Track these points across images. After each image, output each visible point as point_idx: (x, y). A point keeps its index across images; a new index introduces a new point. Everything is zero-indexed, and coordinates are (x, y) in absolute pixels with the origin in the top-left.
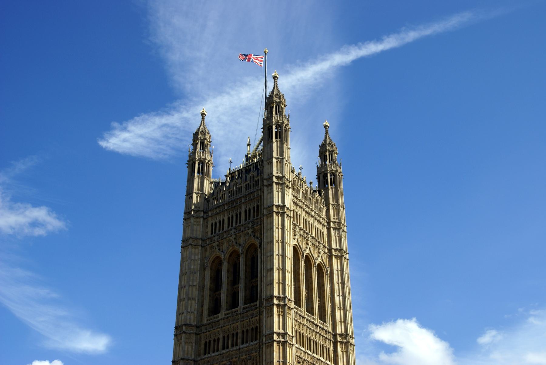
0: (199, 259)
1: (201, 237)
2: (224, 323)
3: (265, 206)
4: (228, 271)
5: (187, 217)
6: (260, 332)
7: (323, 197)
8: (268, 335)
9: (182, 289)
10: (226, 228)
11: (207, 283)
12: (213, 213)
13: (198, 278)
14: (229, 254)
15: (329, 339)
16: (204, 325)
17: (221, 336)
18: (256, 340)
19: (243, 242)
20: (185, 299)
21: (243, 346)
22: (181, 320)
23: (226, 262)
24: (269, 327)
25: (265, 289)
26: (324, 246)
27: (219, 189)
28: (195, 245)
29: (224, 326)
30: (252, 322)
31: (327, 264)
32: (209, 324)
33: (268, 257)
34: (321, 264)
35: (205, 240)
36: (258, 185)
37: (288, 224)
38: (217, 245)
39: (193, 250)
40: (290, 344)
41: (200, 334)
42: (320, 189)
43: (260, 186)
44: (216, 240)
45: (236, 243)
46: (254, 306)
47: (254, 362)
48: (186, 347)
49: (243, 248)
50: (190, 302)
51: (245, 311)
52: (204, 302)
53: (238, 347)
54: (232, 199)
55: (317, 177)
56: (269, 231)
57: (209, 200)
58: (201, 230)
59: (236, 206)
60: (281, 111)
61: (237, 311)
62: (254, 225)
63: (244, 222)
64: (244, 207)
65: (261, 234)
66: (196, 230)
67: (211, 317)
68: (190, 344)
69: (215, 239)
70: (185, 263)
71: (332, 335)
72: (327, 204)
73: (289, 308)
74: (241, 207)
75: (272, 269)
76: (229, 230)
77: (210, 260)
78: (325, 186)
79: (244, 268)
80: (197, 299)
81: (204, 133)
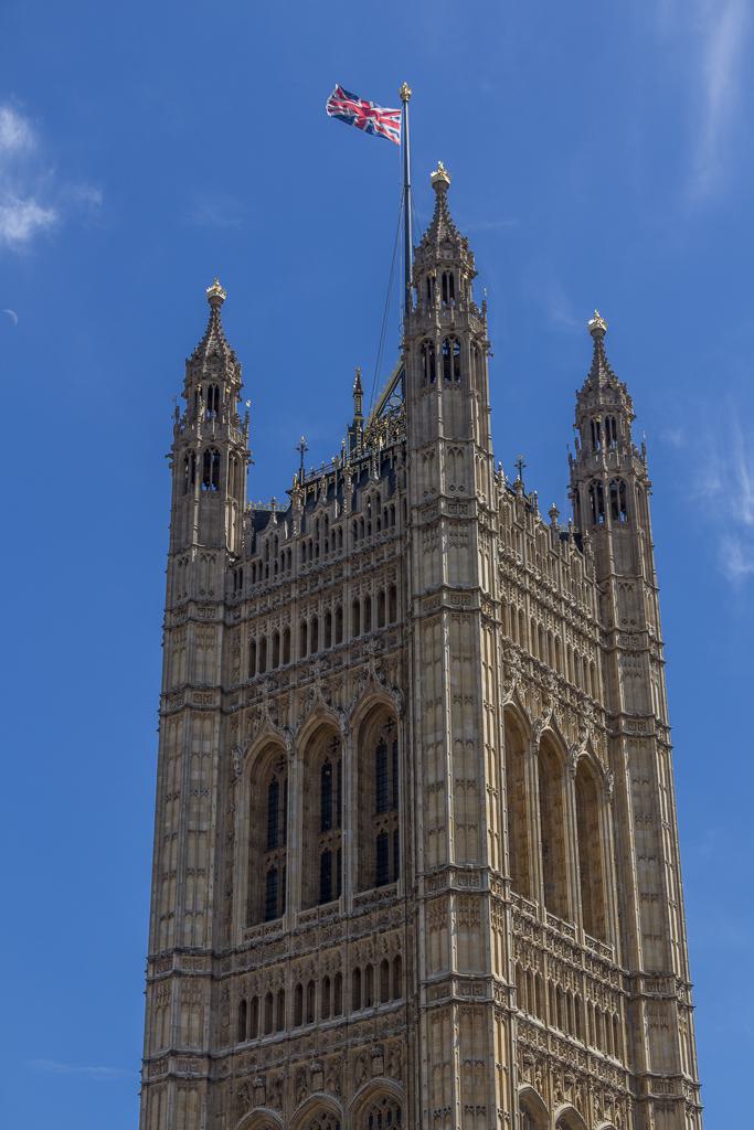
0: (216, 752)
1: (219, 684)
2: (298, 946)
3: (417, 592)
4: (306, 789)
5: (173, 620)
6: (409, 974)
7: (592, 553)
8: (434, 983)
9: (168, 844)
10: (295, 658)
11: (242, 823)
12: (255, 610)
13: (214, 810)
14: (308, 736)
15: (614, 991)
16: (236, 952)
17: (289, 986)
18: (397, 997)
19: (350, 701)
20: (175, 872)
21: (357, 1015)
22: (167, 936)
23: (299, 760)
24: (435, 958)
25: (421, 846)
26: (597, 709)
27: (272, 534)
28: (203, 710)
29: (297, 956)
30: (382, 944)
31: (604, 761)
32: (252, 948)
33: (429, 747)
34: (586, 762)
35: (231, 692)
36: (393, 523)
37: (486, 642)
38: (271, 709)
39: (197, 723)
40: (502, 1009)
41: (224, 978)
42: (580, 530)
43: (397, 527)
44: (265, 691)
45: (329, 703)
46: (389, 894)
47: (394, 1064)
48: (185, 1017)
49: (351, 719)
50: (190, 881)
51: (361, 910)
52: (235, 881)
53: (341, 1020)
54: (314, 567)
55: (570, 491)
56: (429, 669)
57: (241, 569)
58: (219, 663)
59: (325, 589)
60: (460, 293)
61: (337, 911)
62: (383, 647)
63: (350, 638)
64: (350, 591)
65: (405, 675)
66: (205, 664)
67: (257, 928)
68: (196, 1008)
69: (264, 689)
70: (172, 762)
71: (625, 977)
72: (603, 579)
73: (496, 901)
74: (341, 592)
75: (441, 785)
76: (305, 663)
77: (249, 754)
78: (595, 521)
79: (356, 780)
80: (212, 872)
81: (217, 358)
